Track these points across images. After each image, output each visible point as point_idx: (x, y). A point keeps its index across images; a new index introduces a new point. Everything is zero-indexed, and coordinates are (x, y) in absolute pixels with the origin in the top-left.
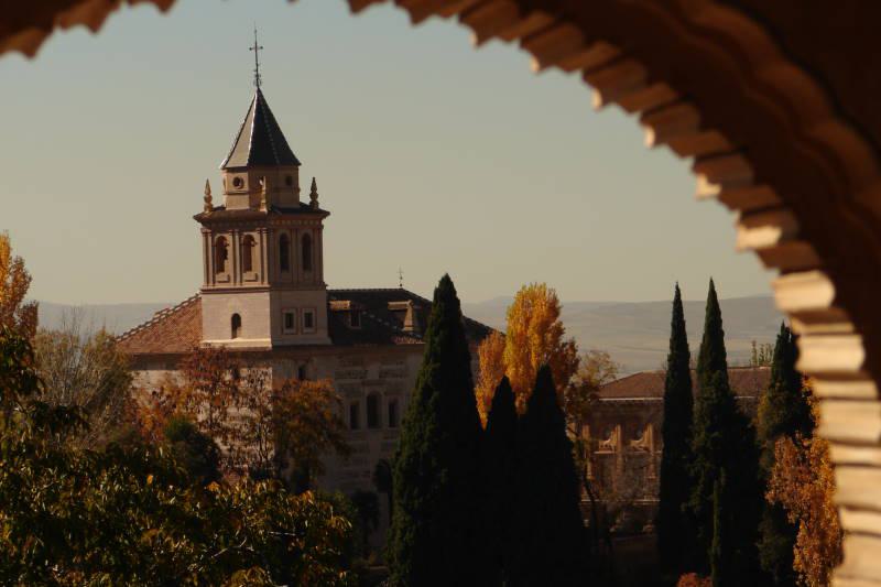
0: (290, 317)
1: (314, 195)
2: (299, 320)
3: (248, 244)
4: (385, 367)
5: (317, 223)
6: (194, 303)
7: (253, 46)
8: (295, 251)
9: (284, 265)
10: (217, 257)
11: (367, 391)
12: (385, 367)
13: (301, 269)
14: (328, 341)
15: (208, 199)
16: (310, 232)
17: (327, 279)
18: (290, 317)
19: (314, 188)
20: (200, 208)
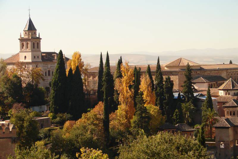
0: (35, 56)
1: (39, 36)
2: (36, 57)
3: (28, 44)
4: (52, 65)
6: (18, 54)
8: (36, 45)
9: (34, 48)
10: (22, 46)
11: (48, 69)
12: (52, 65)
14: (42, 61)
15: (21, 36)
16: (38, 42)
17: (41, 50)
18: (35, 56)
19: (39, 34)
20: (19, 38)
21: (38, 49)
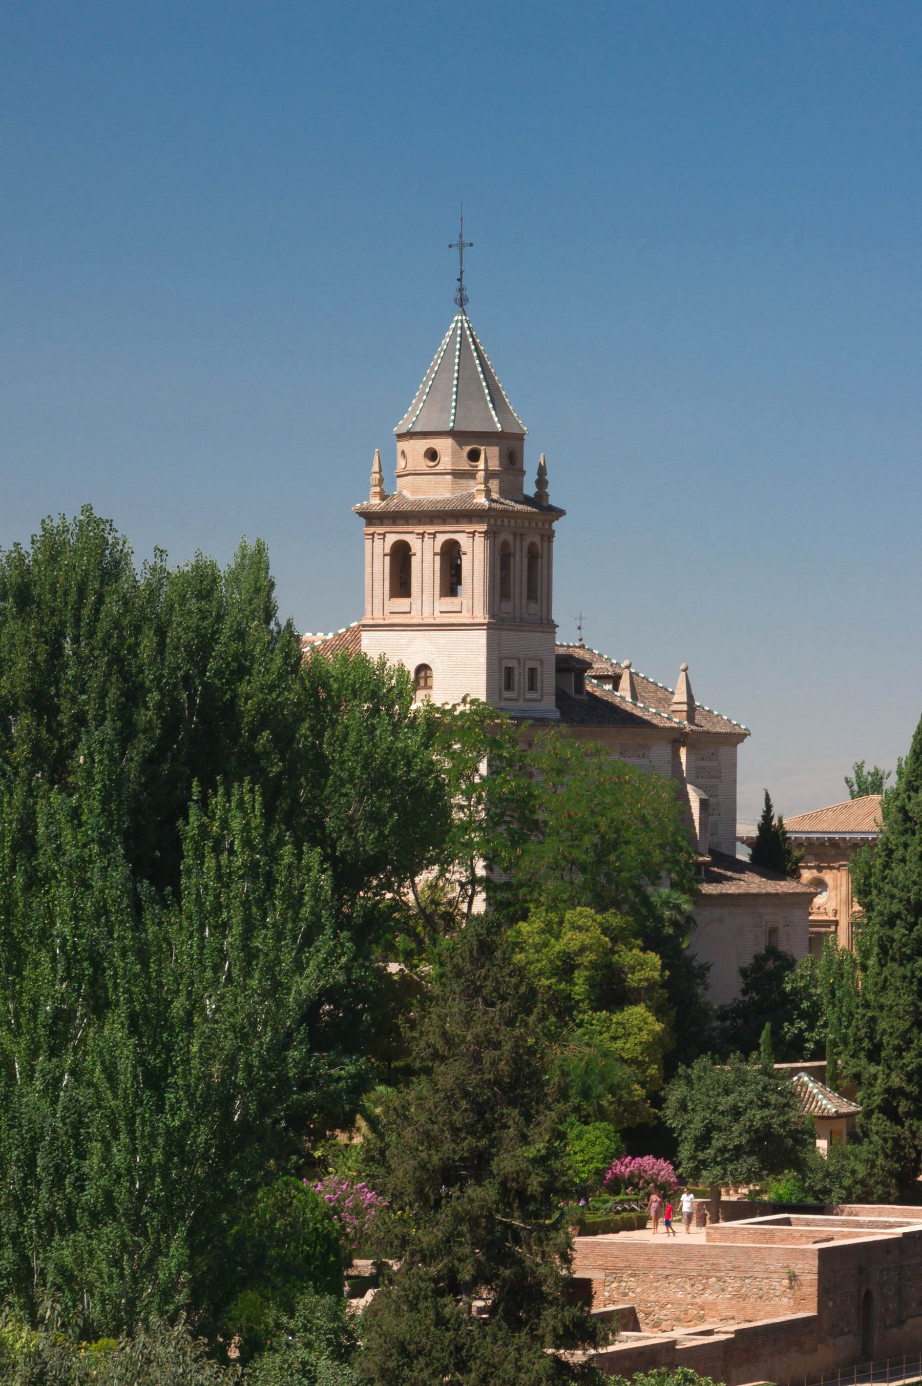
0: (509, 671)
1: (541, 482)
2: (521, 679)
5: (547, 526)
7: (455, 240)
8: (519, 564)
13: (524, 601)
14: (557, 715)
16: (537, 540)
18: (509, 671)
19: (542, 471)
21: (533, 608)
